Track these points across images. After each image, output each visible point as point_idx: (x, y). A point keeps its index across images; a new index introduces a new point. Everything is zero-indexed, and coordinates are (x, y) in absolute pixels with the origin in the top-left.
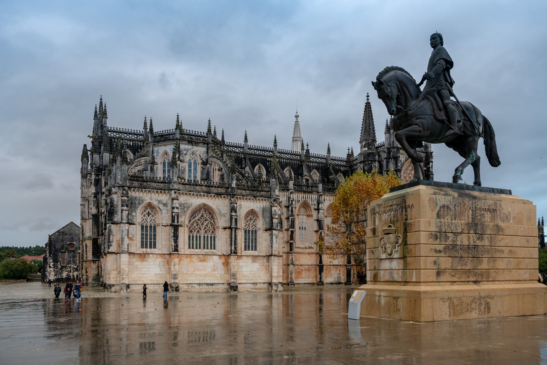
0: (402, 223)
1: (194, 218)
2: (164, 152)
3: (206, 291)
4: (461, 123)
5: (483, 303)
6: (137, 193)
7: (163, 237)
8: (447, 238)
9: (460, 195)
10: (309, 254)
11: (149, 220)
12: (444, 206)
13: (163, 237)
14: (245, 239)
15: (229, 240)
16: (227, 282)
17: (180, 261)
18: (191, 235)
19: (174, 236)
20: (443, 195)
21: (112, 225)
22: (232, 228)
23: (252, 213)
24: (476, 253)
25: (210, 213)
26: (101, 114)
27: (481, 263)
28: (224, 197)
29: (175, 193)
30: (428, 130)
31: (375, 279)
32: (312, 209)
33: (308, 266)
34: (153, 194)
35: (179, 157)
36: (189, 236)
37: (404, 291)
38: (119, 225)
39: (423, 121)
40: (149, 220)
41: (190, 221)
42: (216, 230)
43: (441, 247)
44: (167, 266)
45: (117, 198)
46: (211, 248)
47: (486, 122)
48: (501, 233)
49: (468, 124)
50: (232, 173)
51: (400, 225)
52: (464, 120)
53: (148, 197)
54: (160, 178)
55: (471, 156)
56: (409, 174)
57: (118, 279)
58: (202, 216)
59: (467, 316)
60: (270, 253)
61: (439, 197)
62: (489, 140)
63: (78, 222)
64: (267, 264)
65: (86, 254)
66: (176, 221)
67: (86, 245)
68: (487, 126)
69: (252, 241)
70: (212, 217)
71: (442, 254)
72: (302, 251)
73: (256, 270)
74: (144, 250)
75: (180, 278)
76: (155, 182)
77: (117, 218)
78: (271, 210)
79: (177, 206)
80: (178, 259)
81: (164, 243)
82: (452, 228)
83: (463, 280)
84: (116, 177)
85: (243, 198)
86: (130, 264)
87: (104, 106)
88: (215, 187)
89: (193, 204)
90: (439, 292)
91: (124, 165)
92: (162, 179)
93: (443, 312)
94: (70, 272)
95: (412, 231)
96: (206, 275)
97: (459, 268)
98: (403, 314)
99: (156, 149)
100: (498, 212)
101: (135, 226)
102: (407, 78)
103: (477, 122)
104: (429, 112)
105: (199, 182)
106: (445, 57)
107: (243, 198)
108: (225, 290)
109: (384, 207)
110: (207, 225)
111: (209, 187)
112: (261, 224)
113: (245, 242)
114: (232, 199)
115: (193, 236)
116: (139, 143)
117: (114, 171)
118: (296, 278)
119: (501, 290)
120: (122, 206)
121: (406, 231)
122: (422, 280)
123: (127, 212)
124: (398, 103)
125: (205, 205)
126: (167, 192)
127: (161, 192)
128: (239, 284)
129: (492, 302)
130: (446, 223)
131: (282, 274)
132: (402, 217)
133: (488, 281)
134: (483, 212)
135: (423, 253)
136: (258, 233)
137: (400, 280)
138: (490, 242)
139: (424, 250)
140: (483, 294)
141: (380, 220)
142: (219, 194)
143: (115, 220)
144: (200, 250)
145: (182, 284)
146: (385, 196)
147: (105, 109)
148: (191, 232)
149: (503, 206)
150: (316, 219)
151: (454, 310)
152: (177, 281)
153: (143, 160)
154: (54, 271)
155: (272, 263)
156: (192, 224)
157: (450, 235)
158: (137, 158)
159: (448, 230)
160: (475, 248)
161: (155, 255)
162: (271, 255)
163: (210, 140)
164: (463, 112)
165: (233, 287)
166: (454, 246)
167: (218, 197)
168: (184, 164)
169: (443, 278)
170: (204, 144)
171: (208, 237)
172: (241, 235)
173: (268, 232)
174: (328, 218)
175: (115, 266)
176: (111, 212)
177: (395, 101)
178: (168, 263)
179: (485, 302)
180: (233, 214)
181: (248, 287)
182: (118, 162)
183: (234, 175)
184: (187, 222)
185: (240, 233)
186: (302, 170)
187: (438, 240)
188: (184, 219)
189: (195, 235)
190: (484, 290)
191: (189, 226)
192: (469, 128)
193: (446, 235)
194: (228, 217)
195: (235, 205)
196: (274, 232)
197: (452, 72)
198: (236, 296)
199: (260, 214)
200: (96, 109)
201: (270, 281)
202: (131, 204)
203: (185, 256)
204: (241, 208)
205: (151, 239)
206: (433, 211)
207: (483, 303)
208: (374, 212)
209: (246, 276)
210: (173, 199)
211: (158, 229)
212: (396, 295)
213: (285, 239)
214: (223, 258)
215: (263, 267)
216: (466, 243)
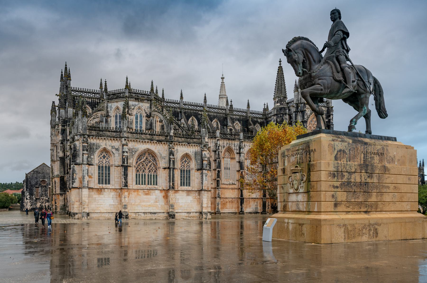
0: (306, 165)
1: (140, 160)
3: (150, 219)
4: (355, 83)
5: (372, 229)
6: (95, 140)
7: (116, 175)
9: (354, 142)
10: (232, 189)
11: (104, 162)
12: (340, 151)
13: (116, 175)
14: (181, 177)
16: (166, 211)
17: (129, 194)
18: (138, 173)
19: (124, 175)
20: (340, 141)
22: (170, 169)
23: (187, 156)
24: (367, 189)
25: (153, 156)
26: (66, 77)
27: (370, 196)
28: (164, 143)
29: (125, 140)
30: (328, 88)
31: (285, 209)
32: (235, 153)
33: (231, 199)
34: (107, 141)
35: (128, 111)
36: (137, 175)
37: (308, 219)
39: (324, 81)
40: (104, 162)
41: (137, 162)
42: (158, 169)
43: (338, 184)
45: (79, 144)
46: (154, 184)
47: (376, 82)
48: (387, 173)
49: (361, 83)
50: (171, 124)
51: (305, 166)
52: (358, 80)
53: (103, 143)
54: (113, 128)
55: (363, 109)
58: (147, 158)
59: (359, 239)
60: (201, 188)
61: (336, 143)
62: (378, 96)
63: (49, 164)
64: (199, 197)
66: (126, 163)
68: (377, 85)
69: (187, 179)
70: (155, 159)
71: (339, 189)
72: (227, 186)
73: (189, 202)
74: (101, 185)
75: (129, 208)
76: (109, 132)
77: (79, 160)
78: (202, 154)
79: (127, 150)
81: (116, 180)
82: (347, 168)
83: (356, 210)
86: (89, 196)
87: (68, 70)
88: (157, 135)
89: (139, 149)
90: (336, 220)
91: (84, 118)
92: (114, 129)
93: (339, 236)
94: (43, 203)
95: (315, 170)
96: (150, 206)
97: (353, 200)
98: (306, 237)
99: (110, 105)
100: (385, 155)
101: (93, 166)
102: (311, 46)
103: (369, 82)
104: (329, 74)
105: (144, 131)
106: (342, 29)
108: (165, 218)
109: (292, 151)
110: (150, 166)
111: (152, 135)
112: (193, 165)
113: (181, 180)
114: (171, 145)
115: (139, 175)
116: (96, 100)
117: (77, 122)
118: (222, 208)
119: (386, 218)
120: (83, 150)
121: (309, 171)
122: (322, 210)
123: (87, 155)
124: (304, 67)
125: (149, 150)
126: (118, 139)
127: (114, 139)
130: (342, 164)
131: (210, 206)
132: (307, 159)
133: (376, 211)
134: (373, 155)
135: (323, 189)
136: (191, 172)
137: (305, 210)
138: (379, 180)
139: (324, 186)
140: (372, 222)
141: (289, 161)
142: (160, 141)
143: (78, 161)
144: (145, 186)
145: (131, 213)
146: (293, 142)
147: (69, 73)
148: (138, 171)
149: (390, 151)
150: (238, 161)
151: (348, 234)
152: (127, 210)
153: (99, 114)
155: (202, 196)
156: (139, 165)
157: (345, 174)
158: (95, 112)
159: (344, 170)
160: (366, 184)
161: (110, 190)
162: (202, 190)
163: (153, 97)
164: (357, 74)
165: (171, 215)
166: (349, 183)
167: (159, 143)
168: (132, 117)
169: (339, 209)
170: (148, 100)
171: (151, 175)
172: (177, 174)
173: (199, 171)
174: (248, 160)
176: (75, 156)
177: (301, 65)
178: (120, 196)
179: (374, 228)
180: (171, 157)
182: (80, 116)
183: (172, 126)
184: (134, 164)
185: (177, 172)
187: (336, 178)
188: (132, 161)
189: (141, 174)
190: (373, 218)
191: (136, 166)
192: (362, 87)
193: (342, 174)
194: (167, 159)
195: (173, 150)
196: (204, 171)
197: (348, 41)
198: (173, 223)
199: (193, 157)
200: (62, 73)
201: (201, 211)
202: (90, 149)
203: (133, 190)
204: (177, 152)
205: (106, 177)
206: (331, 154)
207: (372, 229)
208: (283, 155)
209: (181, 207)
210: (123, 145)
211: (112, 169)
212: (301, 222)
213: (213, 177)
214: (164, 192)
215: (195, 200)
216: (358, 180)
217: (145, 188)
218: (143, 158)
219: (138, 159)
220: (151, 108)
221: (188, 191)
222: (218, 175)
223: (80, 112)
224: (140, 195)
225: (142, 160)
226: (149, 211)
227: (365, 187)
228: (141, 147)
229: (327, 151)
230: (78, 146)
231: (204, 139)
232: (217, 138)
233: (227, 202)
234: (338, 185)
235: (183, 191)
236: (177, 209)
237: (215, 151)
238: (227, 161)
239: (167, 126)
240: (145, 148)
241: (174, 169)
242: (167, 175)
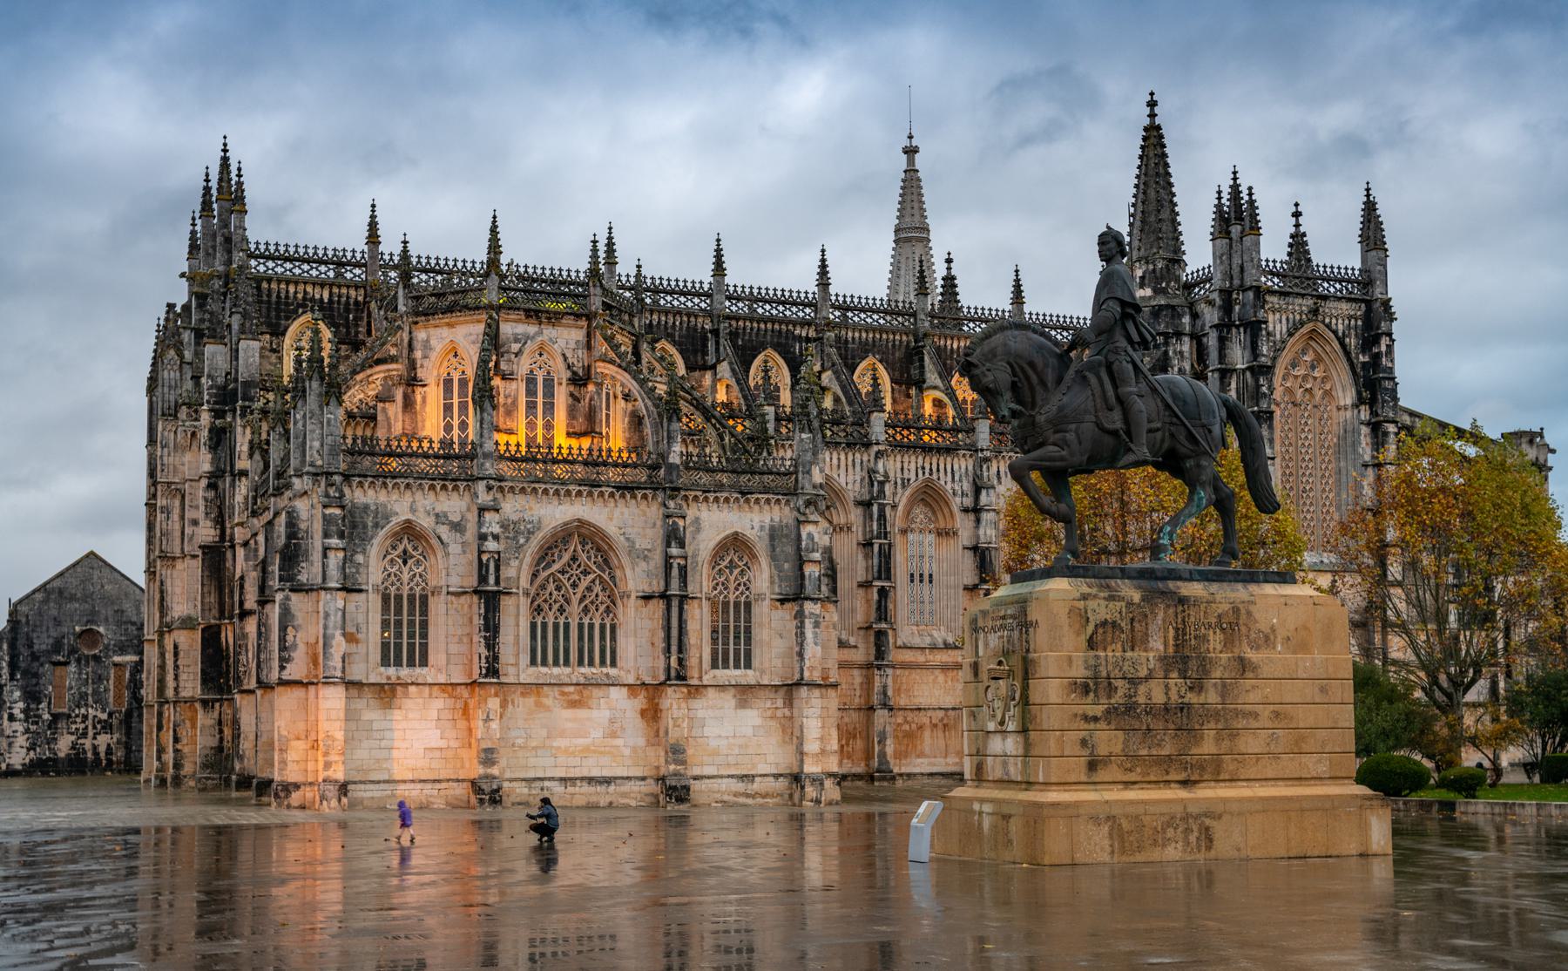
1: (548, 566)
2: (448, 346)
5: (1195, 828)
6: (371, 492)
8: (1111, 689)
10: (945, 668)
11: (406, 577)
12: (1104, 623)
15: (661, 634)
16: (653, 773)
17: (504, 705)
18: (539, 620)
19: (487, 629)
21: (294, 597)
22: (671, 599)
23: (735, 544)
25: (599, 550)
28: (645, 497)
29: (489, 488)
32: (956, 509)
33: (941, 714)
34: (419, 495)
35: (497, 364)
36: (533, 626)
37: (1021, 802)
38: (314, 594)
40: (406, 577)
41: (535, 576)
42: (619, 601)
43: (1098, 710)
44: (462, 724)
45: (309, 510)
46: (603, 663)
50: (670, 420)
51: (1016, 661)
53: (402, 505)
56: (1305, 378)
57: (310, 766)
58: (574, 559)
59: (1155, 855)
60: (797, 676)
61: (1092, 604)
64: (788, 713)
65: (176, 678)
66: (492, 580)
67: (176, 647)
69: (737, 637)
70: (606, 561)
71: (1102, 725)
72: (920, 658)
73: (750, 732)
74: (392, 671)
75: (503, 762)
76: (426, 456)
77: (309, 572)
78: (799, 536)
79: (496, 529)
80: (497, 700)
81: (454, 648)
84: (304, 443)
85: (706, 499)
86: (350, 716)
88: (616, 465)
89: (545, 522)
91: (331, 408)
93: (1096, 846)
96: (586, 751)
97: (1144, 752)
98: (1017, 851)
100: (1243, 629)
101: (363, 596)
106: (1119, 294)
107: (706, 499)
108: (649, 799)
110: (589, 589)
111: (596, 464)
112: (763, 579)
113: (714, 641)
114: (671, 504)
115: (544, 625)
117: (300, 424)
118: (899, 755)
119: (1241, 800)
120: (326, 535)
121: (1026, 677)
123: (341, 555)
126: (462, 485)
127: (444, 487)
128: (695, 778)
129: (1218, 828)
133: (1217, 781)
136: (755, 610)
138: (1223, 697)
140: (1192, 809)
141: (986, 645)
142: (626, 489)
143: (303, 578)
144: (568, 670)
145: (511, 780)
149: (1257, 615)
150: (967, 543)
151: (1122, 841)
153: (379, 374)
154: (27, 731)
155: (800, 709)
156: (543, 587)
157: (1119, 683)
162: (798, 684)
163: (596, 303)
165: (674, 788)
166: (1130, 708)
168: (514, 385)
170: (578, 316)
171: (591, 626)
173: (788, 605)
175: (301, 726)
176: (292, 555)
179: (1201, 827)
180: (674, 551)
181: (723, 787)
182: (312, 400)
183: (676, 426)
184: (524, 582)
185: (697, 612)
186: (922, 367)
188: (518, 572)
189: (551, 621)
190: (1198, 800)
191: (533, 592)
192: (1186, 443)
194: (657, 559)
195: (681, 523)
196: (809, 607)
201: (796, 770)
202: (352, 528)
203: (520, 689)
204: (698, 530)
205: (411, 636)
209: (716, 753)
210: (482, 510)
211: (437, 606)
213: (860, 618)
214: (644, 693)
215: (773, 723)
216: (1159, 698)
217: (567, 680)
218: (560, 557)
219: (538, 564)
220: (589, 347)
221: (745, 692)
222: (879, 608)
223: (315, 384)
224: (548, 709)
225: (556, 567)
226: (586, 773)
227: (1181, 717)
228: (554, 513)
229: (1066, 628)
230: (304, 515)
231: (809, 472)
232: (875, 448)
233: (921, 728)
234: (1099, 714)
235: (721, 687)
236: (700, 764)
237: (866, 505)
238: (921, 544)
239: (657, 426)
240: (568, 518)
241: (683, 599)
242: (659, 622)
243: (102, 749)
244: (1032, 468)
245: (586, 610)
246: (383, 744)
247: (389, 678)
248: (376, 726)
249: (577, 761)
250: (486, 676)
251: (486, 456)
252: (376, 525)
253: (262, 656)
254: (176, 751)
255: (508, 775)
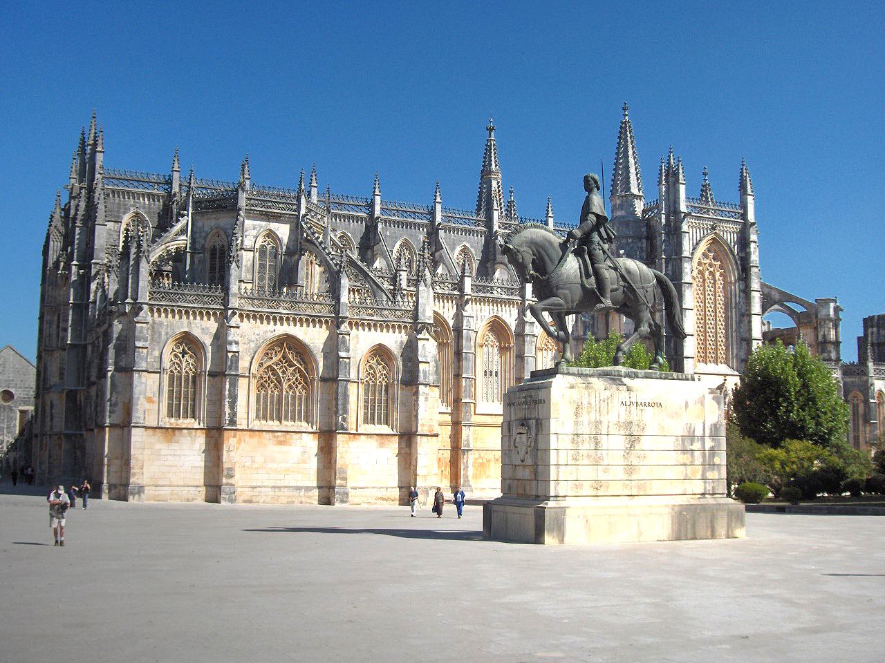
11: (184, 365)
23: (380, 352)
36: (258, 397)
58: (284, 357)
64: (408, 451)
67: (51, 402)
74: (173, 420)
113: (366, 407)
118: (476, 477)
142: (313, 320)
180: (342, 354)
243: (11, 461)
244: (544, 310)
245: (290, 387)
246: (167, 463)
247: (171, 424)
248: (163, 452)
249: (282, 477)
250: (229, 425)
251: (235, 295)
252: (167, 333)
253: (98, 409)
254: (49, 463)
255: (240, 484)
